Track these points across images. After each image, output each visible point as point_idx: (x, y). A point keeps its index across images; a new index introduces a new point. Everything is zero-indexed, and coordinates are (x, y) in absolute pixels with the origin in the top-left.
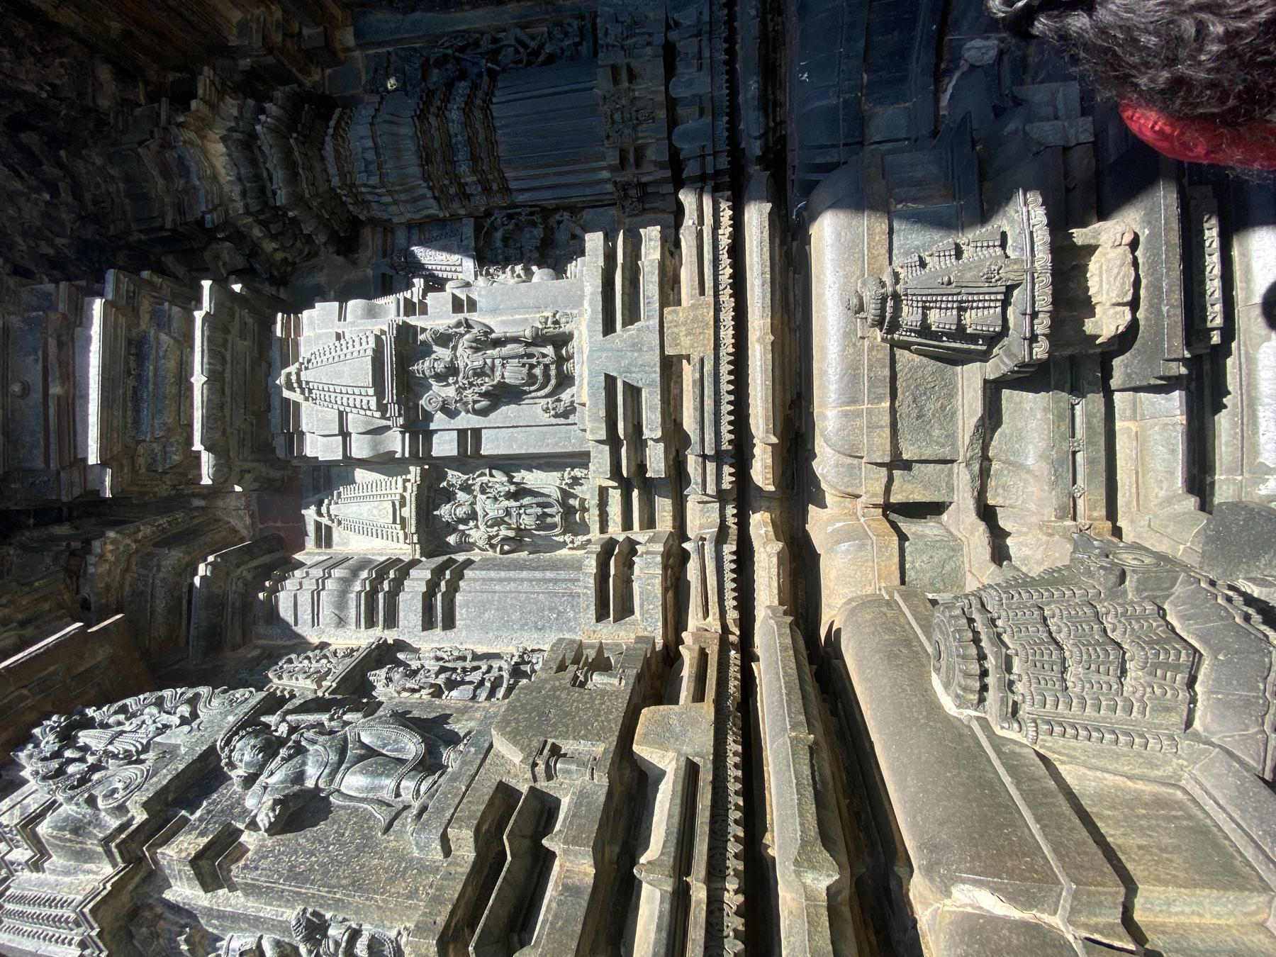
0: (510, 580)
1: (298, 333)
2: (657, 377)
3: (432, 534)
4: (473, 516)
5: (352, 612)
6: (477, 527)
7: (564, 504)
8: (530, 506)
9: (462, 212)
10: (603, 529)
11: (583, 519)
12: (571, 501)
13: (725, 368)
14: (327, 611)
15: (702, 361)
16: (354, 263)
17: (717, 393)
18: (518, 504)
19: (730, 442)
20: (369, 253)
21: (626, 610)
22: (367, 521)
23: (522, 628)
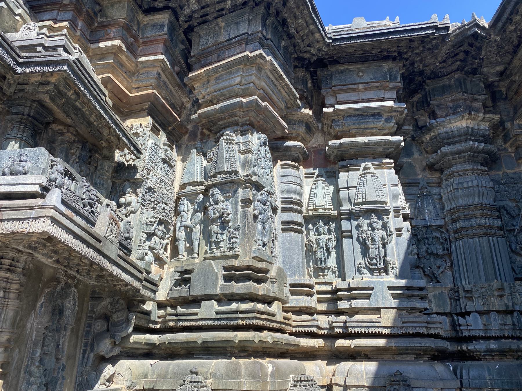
0: (299, 250)
1: (385, 168)
2: (374, 306)
3: (311, 220)
4: (319, 234)
5: (286, 196)
6: (315, 235)
7: (325, 268)
8: (324, 256)
9: (446, 220)
10: (317, 283)
11: (320, 276)
12: (326, 271)
13: (377, 330)
14: (286, 187)
15: (379, 322)
16: (424, 169)
17: (368, 327)
18: (325, 251)
19: (351, 331)
20: (429, 176)
21: (293, 293)
22: (317, 194)
23: (283, 256)
